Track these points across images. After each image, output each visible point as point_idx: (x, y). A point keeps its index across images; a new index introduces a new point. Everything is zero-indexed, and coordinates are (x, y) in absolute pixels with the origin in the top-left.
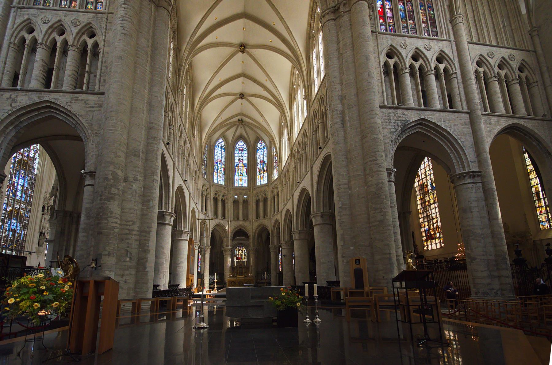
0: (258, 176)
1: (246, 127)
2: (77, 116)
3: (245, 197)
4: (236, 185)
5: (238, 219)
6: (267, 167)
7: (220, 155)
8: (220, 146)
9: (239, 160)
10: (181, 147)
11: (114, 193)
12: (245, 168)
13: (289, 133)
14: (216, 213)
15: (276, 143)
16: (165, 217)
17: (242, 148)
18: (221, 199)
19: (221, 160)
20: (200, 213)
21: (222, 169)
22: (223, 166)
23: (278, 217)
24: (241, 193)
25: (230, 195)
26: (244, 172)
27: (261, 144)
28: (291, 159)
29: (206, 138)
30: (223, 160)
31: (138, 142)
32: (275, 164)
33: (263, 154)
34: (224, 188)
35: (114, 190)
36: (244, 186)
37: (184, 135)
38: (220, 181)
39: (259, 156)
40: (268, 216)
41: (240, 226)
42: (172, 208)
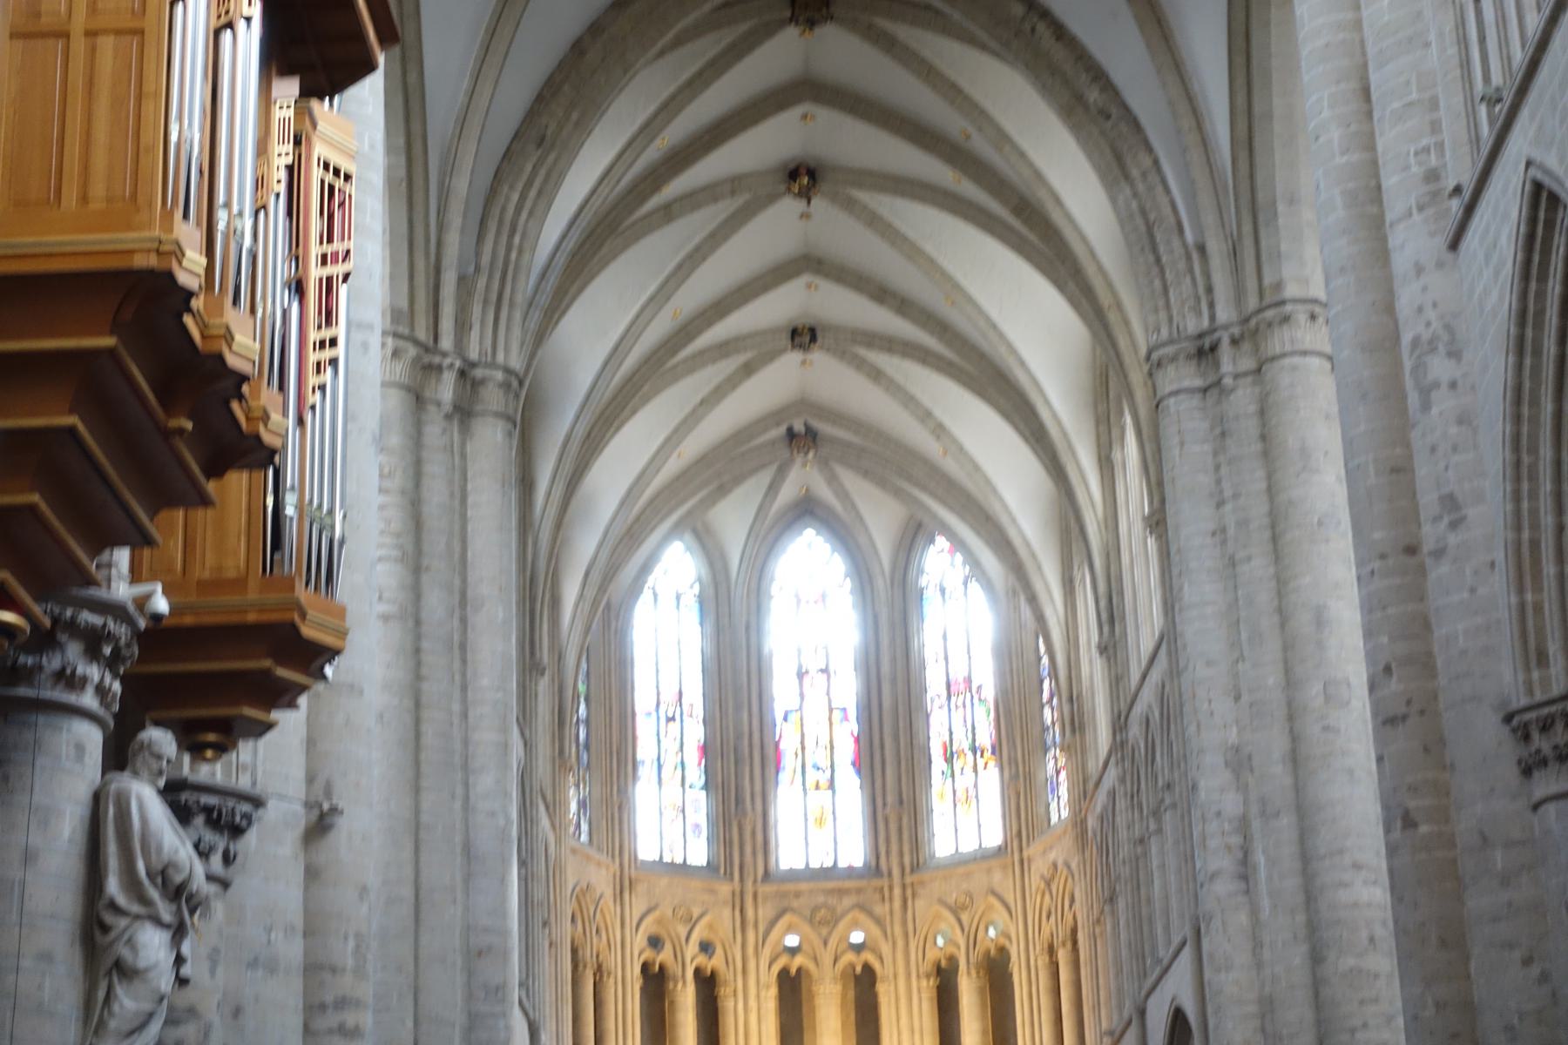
13: (1104, 616)
21: (693, 756)
22: (696, 733)
28: (1122, 780)
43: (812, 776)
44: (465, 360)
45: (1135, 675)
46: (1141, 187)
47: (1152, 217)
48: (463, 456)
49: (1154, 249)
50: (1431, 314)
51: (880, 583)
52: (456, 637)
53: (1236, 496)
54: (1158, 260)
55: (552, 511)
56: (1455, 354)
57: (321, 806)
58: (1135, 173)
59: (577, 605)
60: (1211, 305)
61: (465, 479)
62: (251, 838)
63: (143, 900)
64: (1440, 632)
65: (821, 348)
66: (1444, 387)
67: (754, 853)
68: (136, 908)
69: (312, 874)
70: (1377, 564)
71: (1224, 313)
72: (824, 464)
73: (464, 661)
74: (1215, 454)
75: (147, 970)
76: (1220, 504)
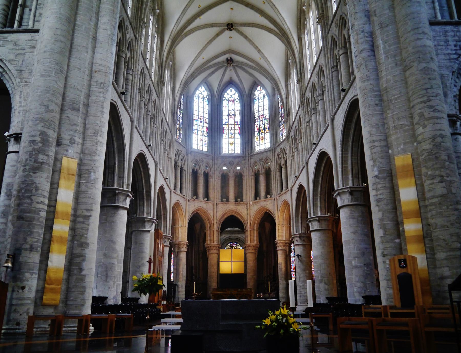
0: (256, 137)
1: (236, 68)
2: (4, 61)
3: (238, 168)
4: (224, 152)
5: (228, 200)
7: (201, 110)
8: (201, 96)
9: (229, 115)
10: (144, 99)
11: (41, 161)
12: (237, 127)
13: (299, 73)
14: (195, 193)
15: (281, 89)
16: (118, 198)
17: (232, 99)
18: (202, 173)
19: (203, 117)
20: (173, 194)
21: (205, 129)
22: (206, 125)
24: (231, 163)
25: (216, 166)
26: (237, 131)
27: (259, 92)
29: (182, 86)
30: (206, 116)
31: (78, 90)
32: (280, 119)
33: (263, 106)
35: (41, 157)
36: (236, 152)
37: (148, 82)
40: (273, 196)
42: (128, 185)
43: (230, 135)
51: (245, 97)
72: (234, 68)
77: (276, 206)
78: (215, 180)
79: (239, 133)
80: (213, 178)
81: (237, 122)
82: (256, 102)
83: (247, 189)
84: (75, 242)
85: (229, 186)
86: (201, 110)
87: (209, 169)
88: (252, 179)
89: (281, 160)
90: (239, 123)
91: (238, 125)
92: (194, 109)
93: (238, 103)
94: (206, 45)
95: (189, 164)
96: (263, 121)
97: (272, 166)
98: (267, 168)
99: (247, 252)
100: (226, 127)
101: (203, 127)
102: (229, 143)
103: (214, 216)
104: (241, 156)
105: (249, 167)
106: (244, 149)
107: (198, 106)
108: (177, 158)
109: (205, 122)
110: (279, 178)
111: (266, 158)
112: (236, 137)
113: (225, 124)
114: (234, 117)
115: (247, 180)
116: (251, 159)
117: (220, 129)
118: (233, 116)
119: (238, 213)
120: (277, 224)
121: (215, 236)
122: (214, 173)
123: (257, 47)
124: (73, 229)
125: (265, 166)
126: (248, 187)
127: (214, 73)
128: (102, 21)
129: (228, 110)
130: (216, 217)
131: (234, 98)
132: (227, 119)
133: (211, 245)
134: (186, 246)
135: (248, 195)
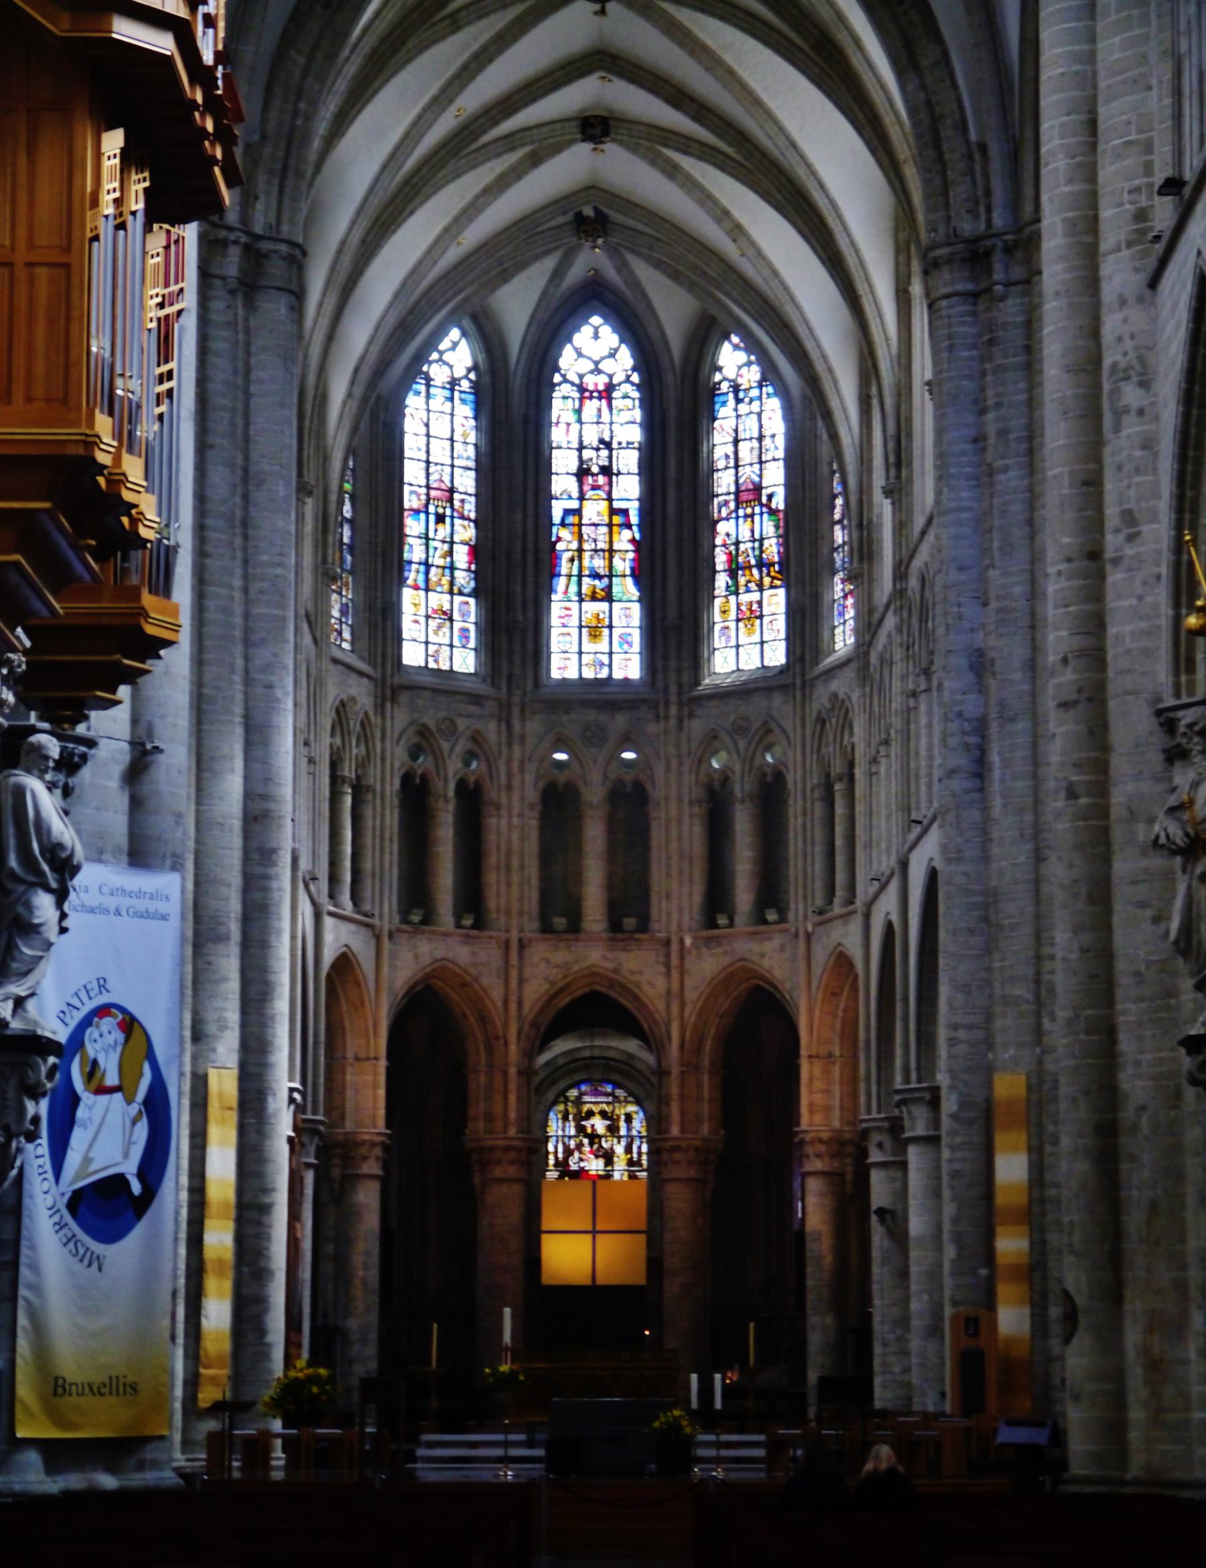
1: (624, 252)
4: (555, 674)
5: (575, 926)
6: (785, 539)
7: (440, 452)
9: (582, 473)
12: (623, 540)
13: (892, 458)
15: (838, 415)
17: (601, 381)
18: (452, 786)
19: (452, 490)
20: (329, 922)
21: (461, 556)
22: (466, 532)
23: (849, 937)
25: (516, 748)
26: (622, 565)
27: (742, 357)
28: (899, 630)
30: (466, 482)
32: (839, 535)
33: (761, 438)
34: (476, 699)
36: (618, 675)
38: (445, 651)
39: (730, 449)
40: (791, 915)
41: (593, 974)
44: (249, 233)
45: (919, 522)
46: (929, 80)
47: (938, 110)
48: (247, 331)
49: (937, 146)
50: (1128, 344)
52: (239, 513)
53: (998, 405)
54: (941, 157)
55: (324, 323)
56: (1145, 385)
57: (143, 744)
58: (925, 63)
59: (344, 403)
60: (989, 210)
61: (248, 353)
62: (86, 773)
63: (42, 874)
64: (1112, 631)
65: (613, 140)
66: (1133, 412)
67: (524, 665)
68: (31, 878)
69: (136, 804)
70: (1062, 567)
71: (998, 221)
72: (613, 251)
73: (245, 537)
74: (982, 359)
75: (40, 925)
76: (983, 412)
77: (802, 966)
78: (515, 821)
79: (633, 569)
80: (504, 813)
81: (625, 512)
82: (725, 412)
83: (669, 866)
84: (245, 1269)
85: (579, 849)
86: (440, 452)
87: (484, 768)
88: (696, 821)
89: (831, 749)
90: (634, 519)
91: (629, 526)
92: (407, 453)
93: (629, 402)
94: (477, 198)
95: (388, 755)
96: (757, 518)
97: (791, 766)
98: (769, 771)
99: (666, 1174)
100: (566, 541)
101: (452, 543)
102: (581, 627)
103: (506, 1002)
104: (644, 701)
105: (680, 757)
106: (659, 663)
107: (428, 435)
108: (338, 741)
109: (462, 517)
110: (819, 834)
111: (765, 723)
112: (615, 589)
113: (563, 524)
114: (610, 484)
115: (668, 822)
116: (691, 715)
117: (537, 551)
118: (601, 480)
119: (622, 986)
120: (803, 1052)
121: (512, 1098)
122: (509, 788)
123: (726, 213)
124: (239, 1239)
125: (757, 762)
126: (674, 860)
127: (512, 276)
128: (257, 662)
129: (581, 442)
130: (520, 1004)
131: (611, 377)
132: (575, 494)
133: (491, 1143)
134: (378, 1151)
135: (674, 904)
